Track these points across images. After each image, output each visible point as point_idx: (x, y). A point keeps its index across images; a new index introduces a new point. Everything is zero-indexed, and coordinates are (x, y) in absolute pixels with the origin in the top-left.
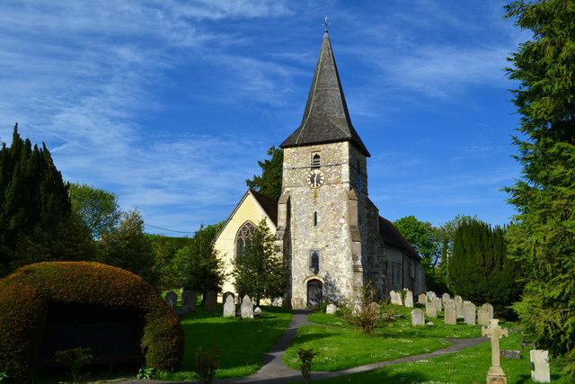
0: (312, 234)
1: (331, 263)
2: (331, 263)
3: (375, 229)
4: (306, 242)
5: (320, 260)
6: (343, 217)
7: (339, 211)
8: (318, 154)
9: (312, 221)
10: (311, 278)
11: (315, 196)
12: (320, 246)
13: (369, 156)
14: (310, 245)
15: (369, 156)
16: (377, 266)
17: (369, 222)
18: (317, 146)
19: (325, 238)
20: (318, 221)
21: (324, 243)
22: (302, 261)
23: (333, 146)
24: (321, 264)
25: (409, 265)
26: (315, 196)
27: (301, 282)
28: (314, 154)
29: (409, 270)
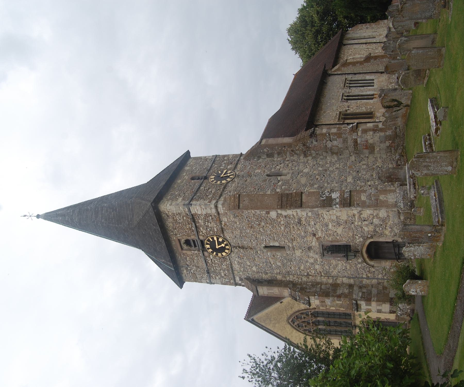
0: (298, 253)
1: (340, 230)
2: (340, 230)
3: (290, 145)
4: (312, 261)
5: (337, 244)
6: (268, 213)
7: (260, 219)
8: (183, 241)
9: (279, 254)
10: (365, 255)
11: (243, 247)
12: (314, 243)
13: (188, 152)
14: (314, 256)
15: (188, 152)
16: (345, 141)
17: (279, 154)
18: (174, 243)
19: (303, 238)
20: (277, 244)
21: (310, 238)
22: (339, 267)
23: (169, 223)
24: (344, 242)
25: (346, 64)
26: (243, 247)
27: (373, 270)
28: (185, 247)
29: (354, 64)
